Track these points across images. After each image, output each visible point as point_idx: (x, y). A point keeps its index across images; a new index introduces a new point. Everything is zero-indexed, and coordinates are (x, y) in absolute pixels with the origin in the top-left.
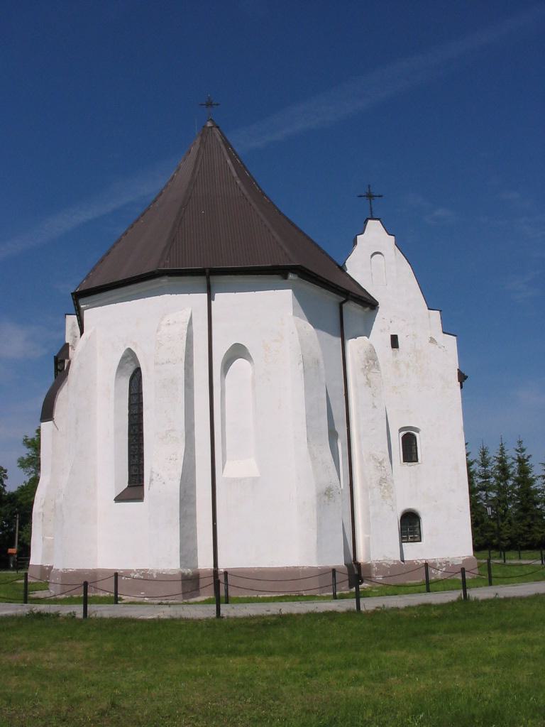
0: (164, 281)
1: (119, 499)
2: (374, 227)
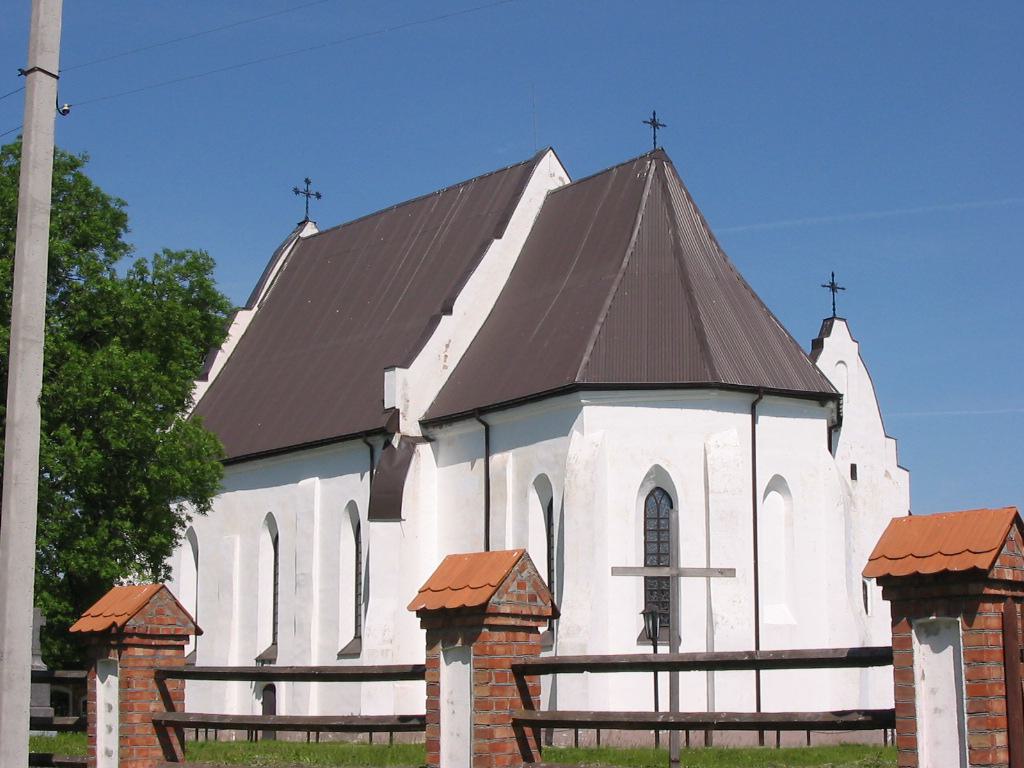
0: (714, 394)
2: (839, 327)
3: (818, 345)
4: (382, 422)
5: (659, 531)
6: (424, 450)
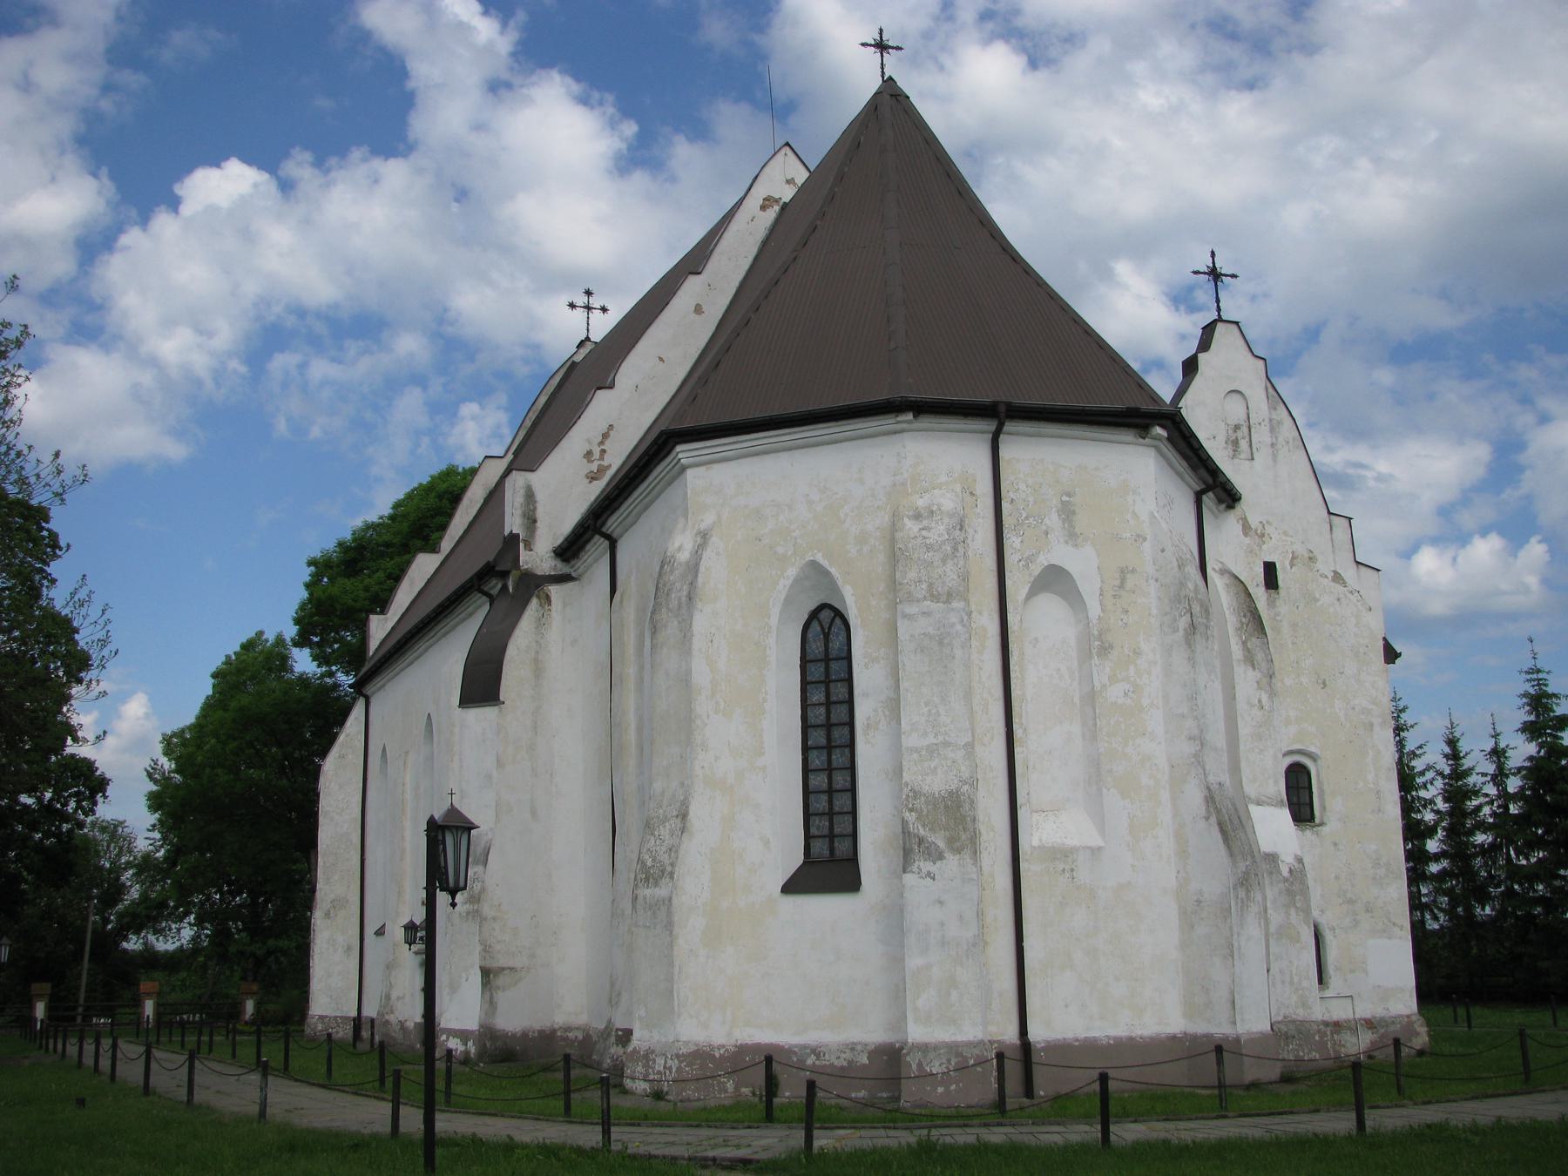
1: (792, 886)
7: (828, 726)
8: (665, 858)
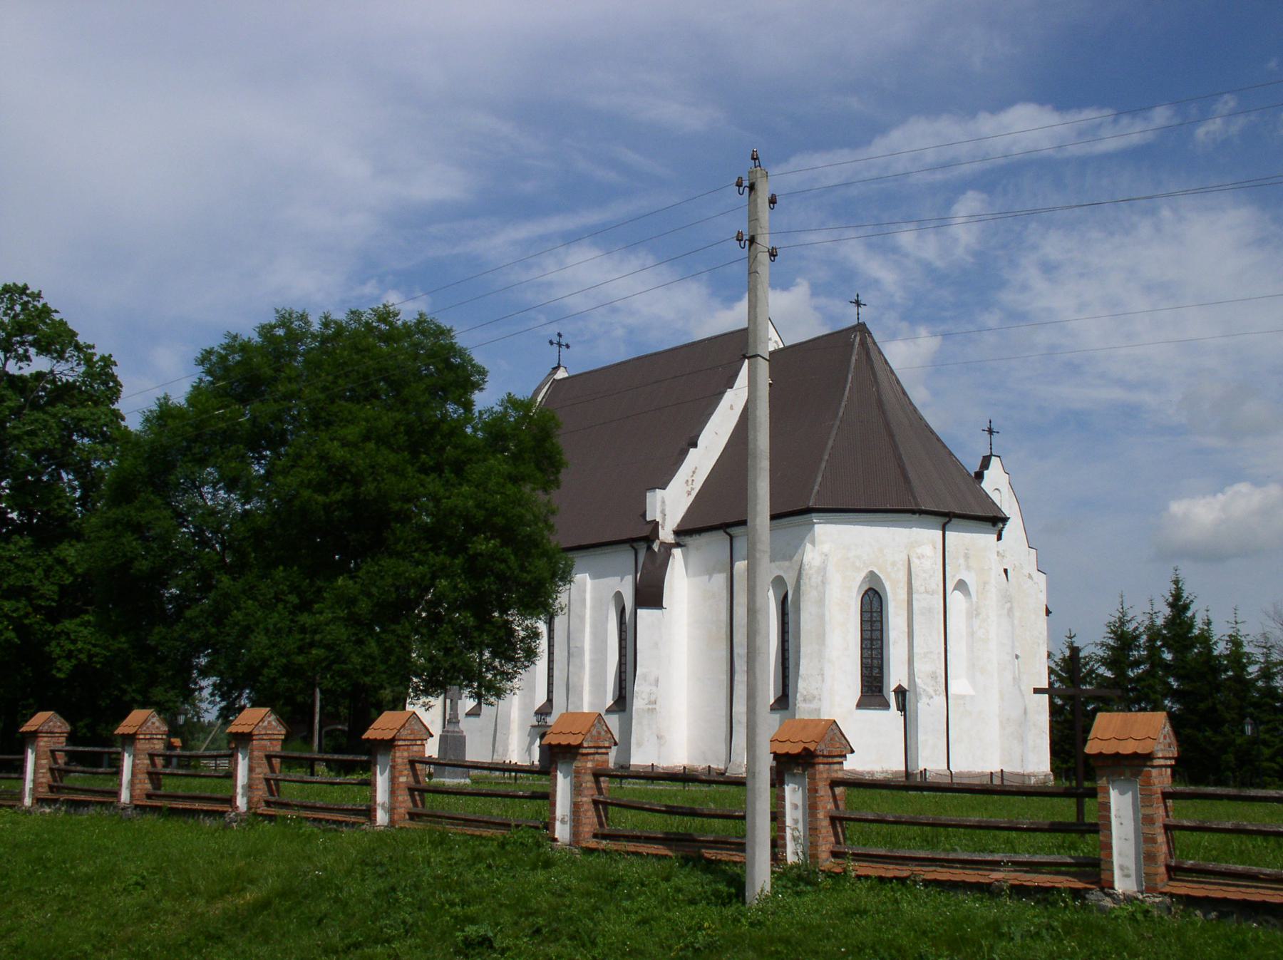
3: (979, 476)
4: (645, 532)
5: (872, 622)
6: (677, 552)
7: (871, 640)
8: (815, 693)
